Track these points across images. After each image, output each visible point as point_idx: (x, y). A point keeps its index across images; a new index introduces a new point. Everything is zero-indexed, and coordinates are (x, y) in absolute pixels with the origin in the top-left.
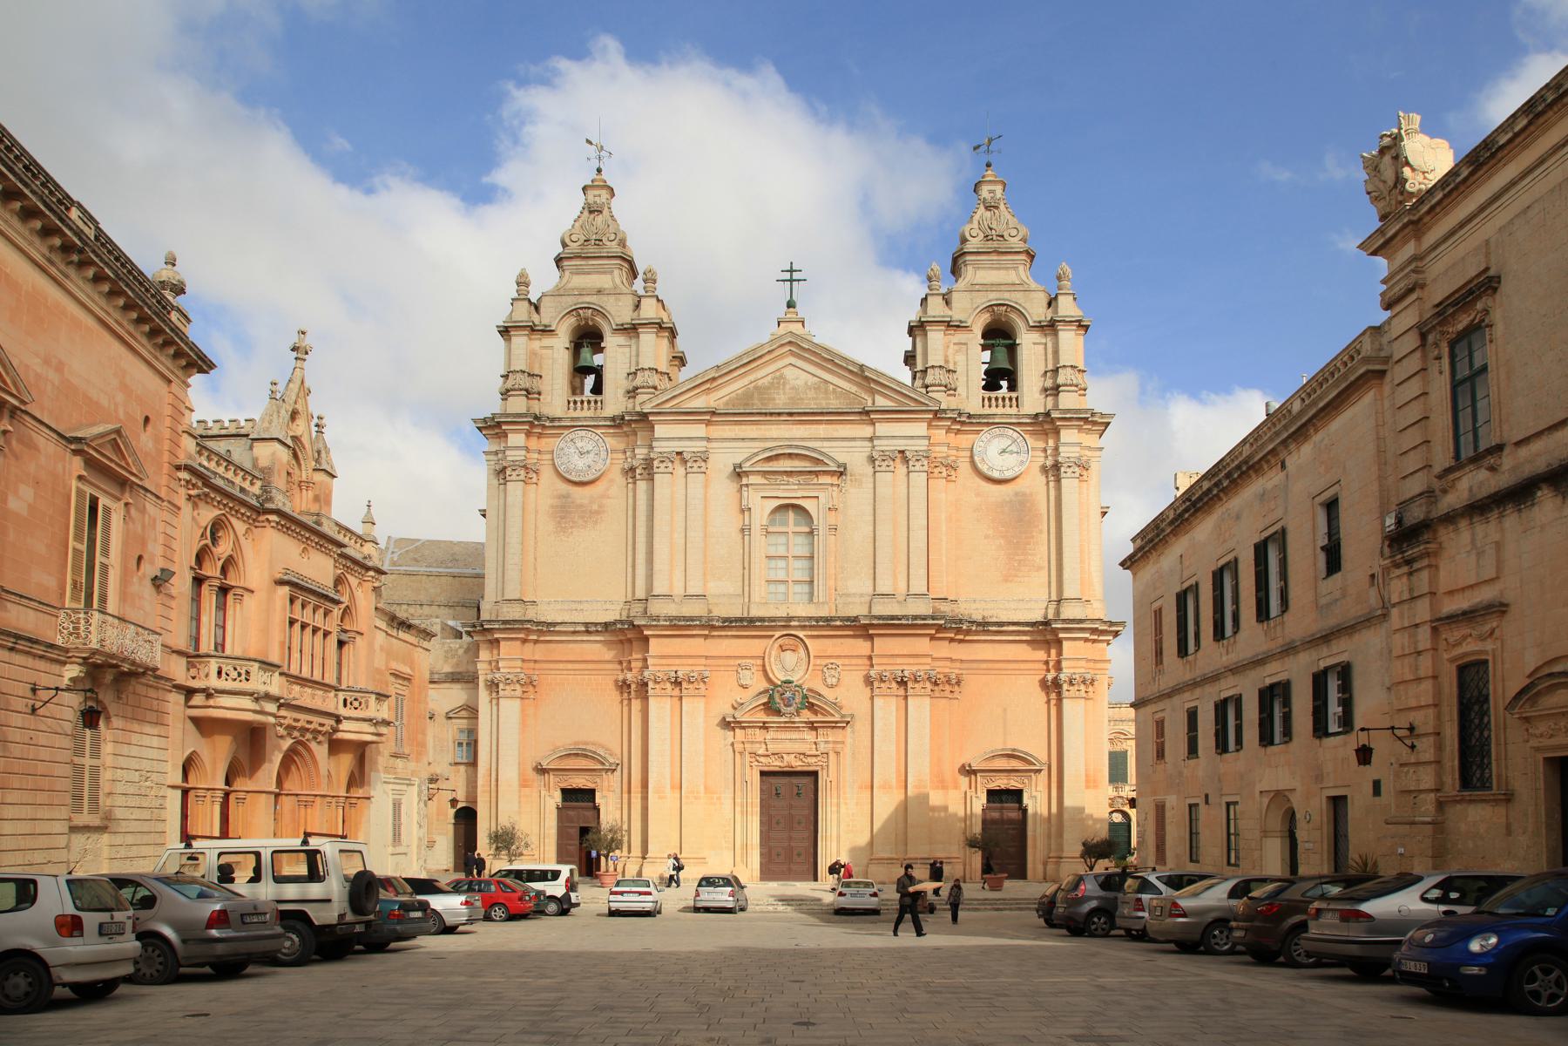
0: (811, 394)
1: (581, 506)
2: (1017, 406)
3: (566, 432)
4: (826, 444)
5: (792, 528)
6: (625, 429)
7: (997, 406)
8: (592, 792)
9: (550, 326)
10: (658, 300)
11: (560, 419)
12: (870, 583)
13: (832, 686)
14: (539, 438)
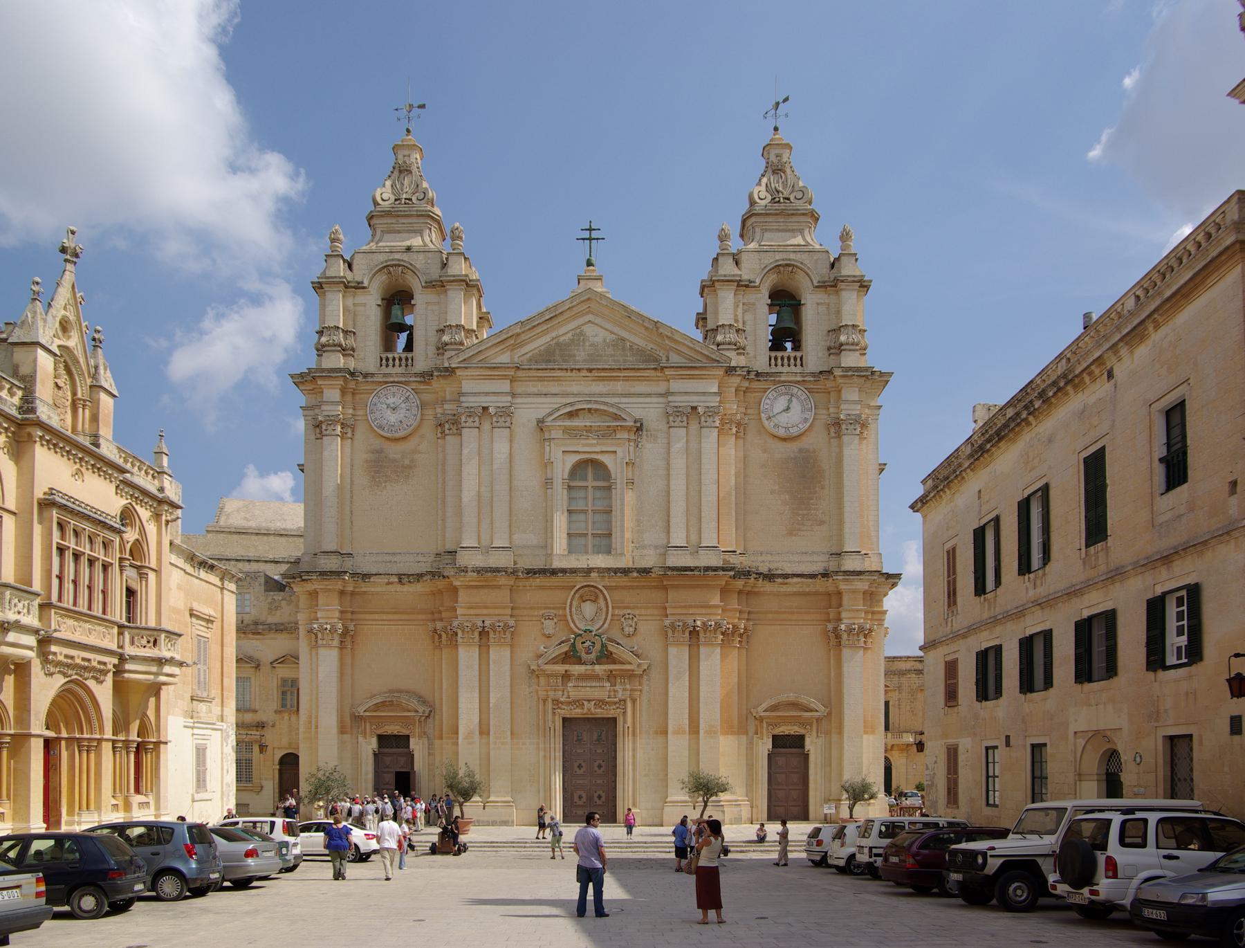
0: (610, 351)
1: (394, 460)
2: (802, 365)
4: (624, 400)
5: (590, 483)
7: (783, 365)
8: (408, 737)
10: (465, 258)
11: (373, 375)
12: (663, 535)
13: (629, 636)
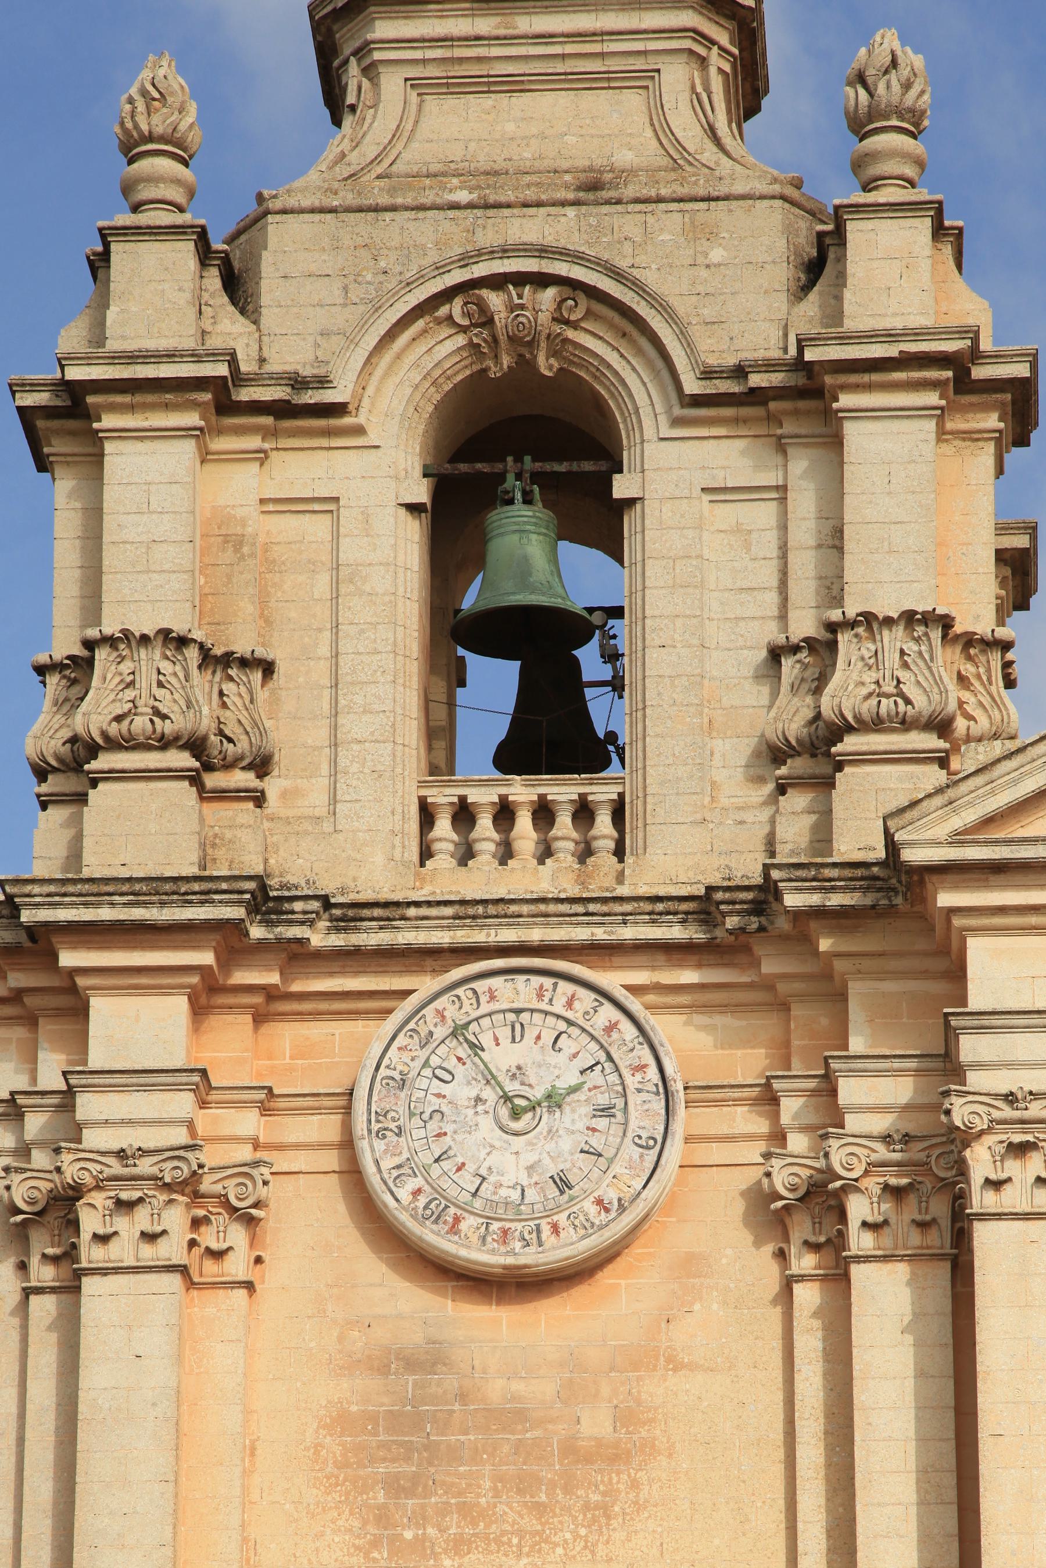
3: (426, 984)
6: (770, 967)
9: (323, 382)
14: (260, 1019)
